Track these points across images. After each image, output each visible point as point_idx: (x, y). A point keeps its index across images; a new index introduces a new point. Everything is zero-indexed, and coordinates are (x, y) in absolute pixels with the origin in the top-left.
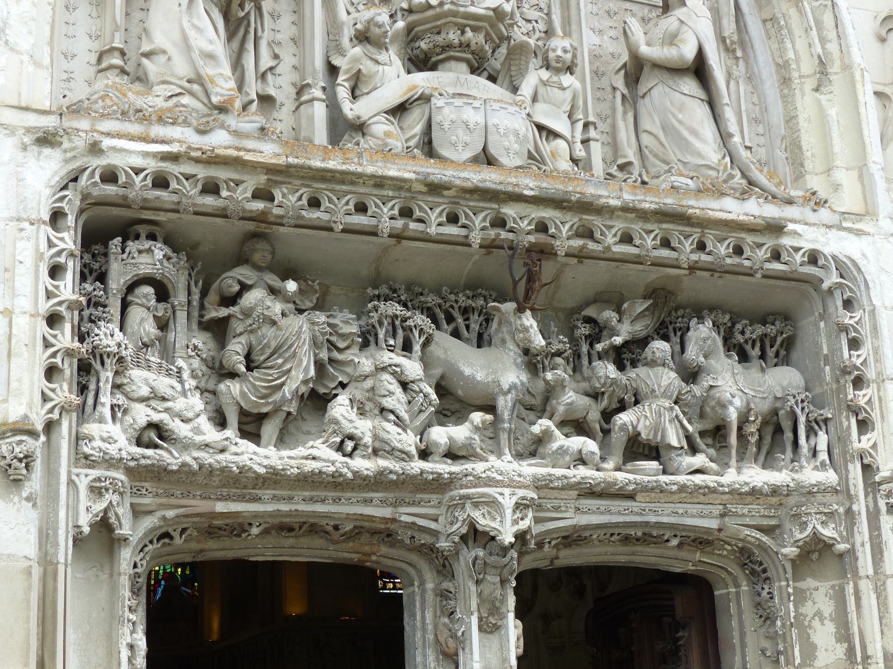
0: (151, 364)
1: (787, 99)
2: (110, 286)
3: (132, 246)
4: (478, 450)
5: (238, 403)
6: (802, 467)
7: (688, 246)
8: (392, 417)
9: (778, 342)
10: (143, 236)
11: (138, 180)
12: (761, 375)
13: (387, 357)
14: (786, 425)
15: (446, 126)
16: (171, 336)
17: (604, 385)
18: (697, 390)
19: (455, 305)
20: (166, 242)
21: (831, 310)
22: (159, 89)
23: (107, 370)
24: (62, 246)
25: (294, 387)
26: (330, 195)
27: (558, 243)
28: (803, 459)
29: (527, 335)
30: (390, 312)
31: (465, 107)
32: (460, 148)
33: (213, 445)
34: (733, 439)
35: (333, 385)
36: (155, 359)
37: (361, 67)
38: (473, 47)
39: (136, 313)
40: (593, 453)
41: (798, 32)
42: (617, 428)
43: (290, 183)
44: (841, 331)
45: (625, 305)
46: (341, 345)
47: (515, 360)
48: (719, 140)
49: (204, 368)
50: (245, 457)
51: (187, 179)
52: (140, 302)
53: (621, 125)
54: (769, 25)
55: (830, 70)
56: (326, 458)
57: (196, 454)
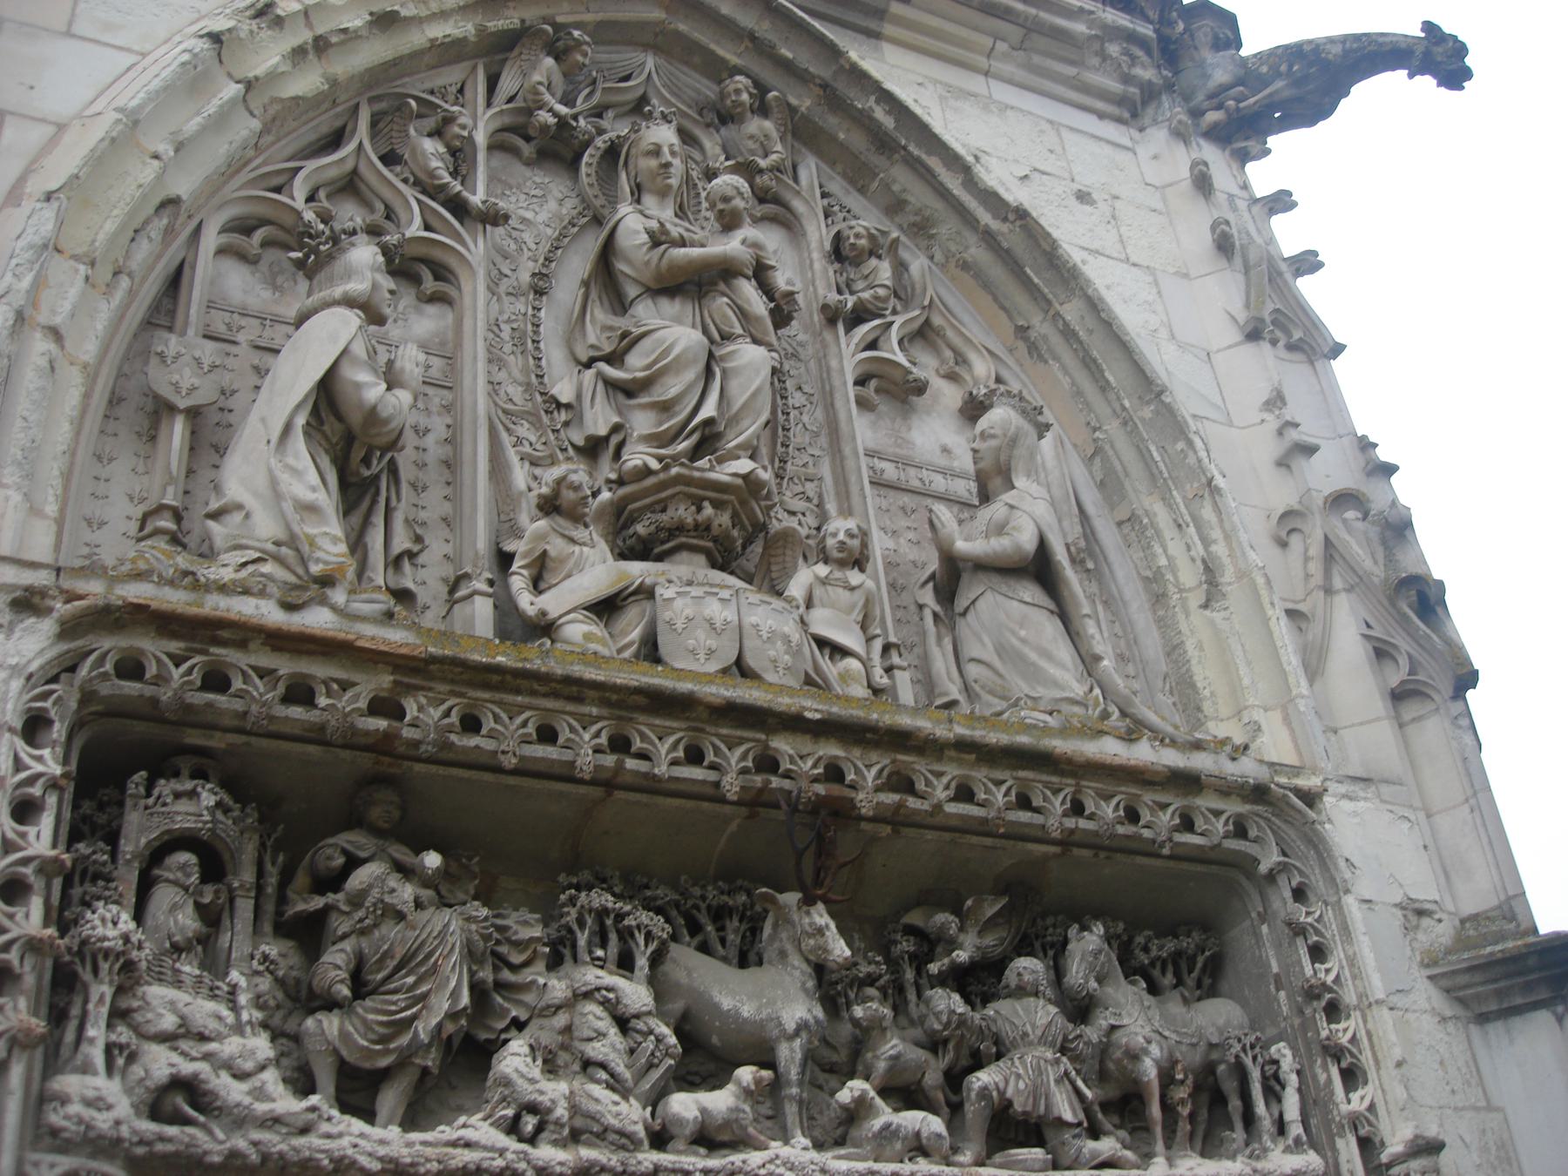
0: (183, 977)
1: (1164, 625)
2: (122, 848)
3: (164, 787)
4: (751, 1130)
5: (336, 1052)
6: (1265, 1150)
7: (1058, 805)
8: (603, 1075)
9: (1199, 965)
10: (185, 772)
11: (176, 673)
12: (1184, 1010)
13: (592, 976)
14: (1230, 1086)
16: (224, 940)
17: (947, 1026)
18: (1092, 1033)
19: (703, 906)
20: (227, 784)
21: (1276, 904)
22: (225, 558)
23: (102, 982)
24: (39, 768)
25: (434, 1022)
26: (497, 710)
27: (861, 796)
28: (1265, 1137)
29: (821, 941)
30: (596, 904)
31: (708, 599)
32: (702, 657)
33: (288, 1120)
34: (1155, 1111)
35: (501, 1025)
36: (189, 969)
38: (715, 531)
39: (163, 896)
40: (939, 1136)
41: (1169, 532)
42: (973, 1095)
43: (430, 689)
44: (1296, 934)
45: (969, 902)
46: (517, 959)
47: (804, 984)
48: (1081, 667)
49: (280, 995)
50: (345, 1141)
51: (261, 678)
52: (171, 876)
53: (935, 651)
54: (1126, 528)
55: (1222, 580)
56: (489, 1144)
57: (256, 1135)
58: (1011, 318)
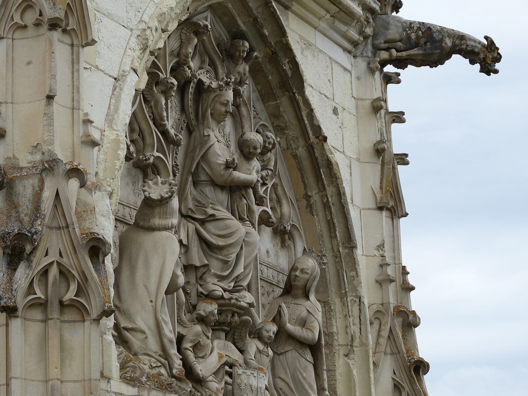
15: (243, 386)
37: (200, 340)
58: (305, 188)
